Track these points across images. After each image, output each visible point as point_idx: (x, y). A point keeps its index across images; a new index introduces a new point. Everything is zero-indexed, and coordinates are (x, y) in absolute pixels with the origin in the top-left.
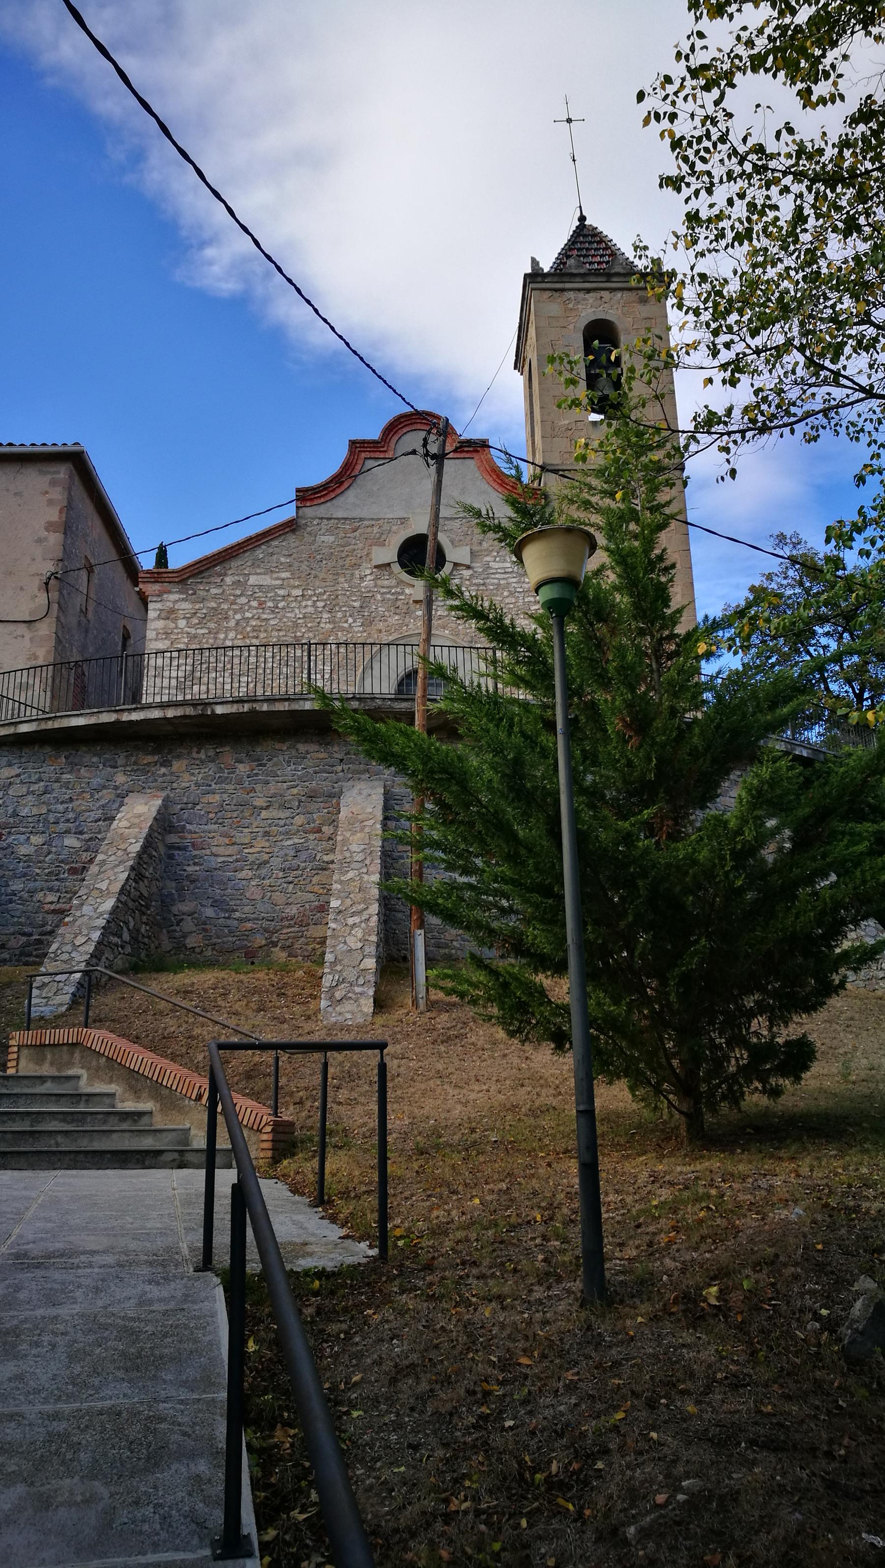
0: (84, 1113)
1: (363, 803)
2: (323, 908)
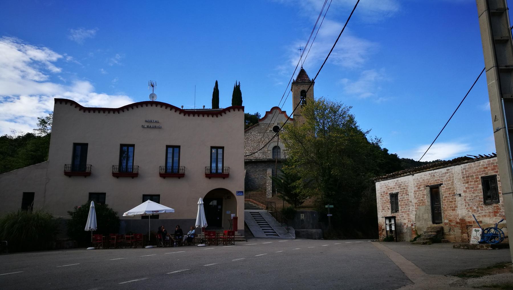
0: (252, 206)
1: (269, 171)
2: (265, 183)
